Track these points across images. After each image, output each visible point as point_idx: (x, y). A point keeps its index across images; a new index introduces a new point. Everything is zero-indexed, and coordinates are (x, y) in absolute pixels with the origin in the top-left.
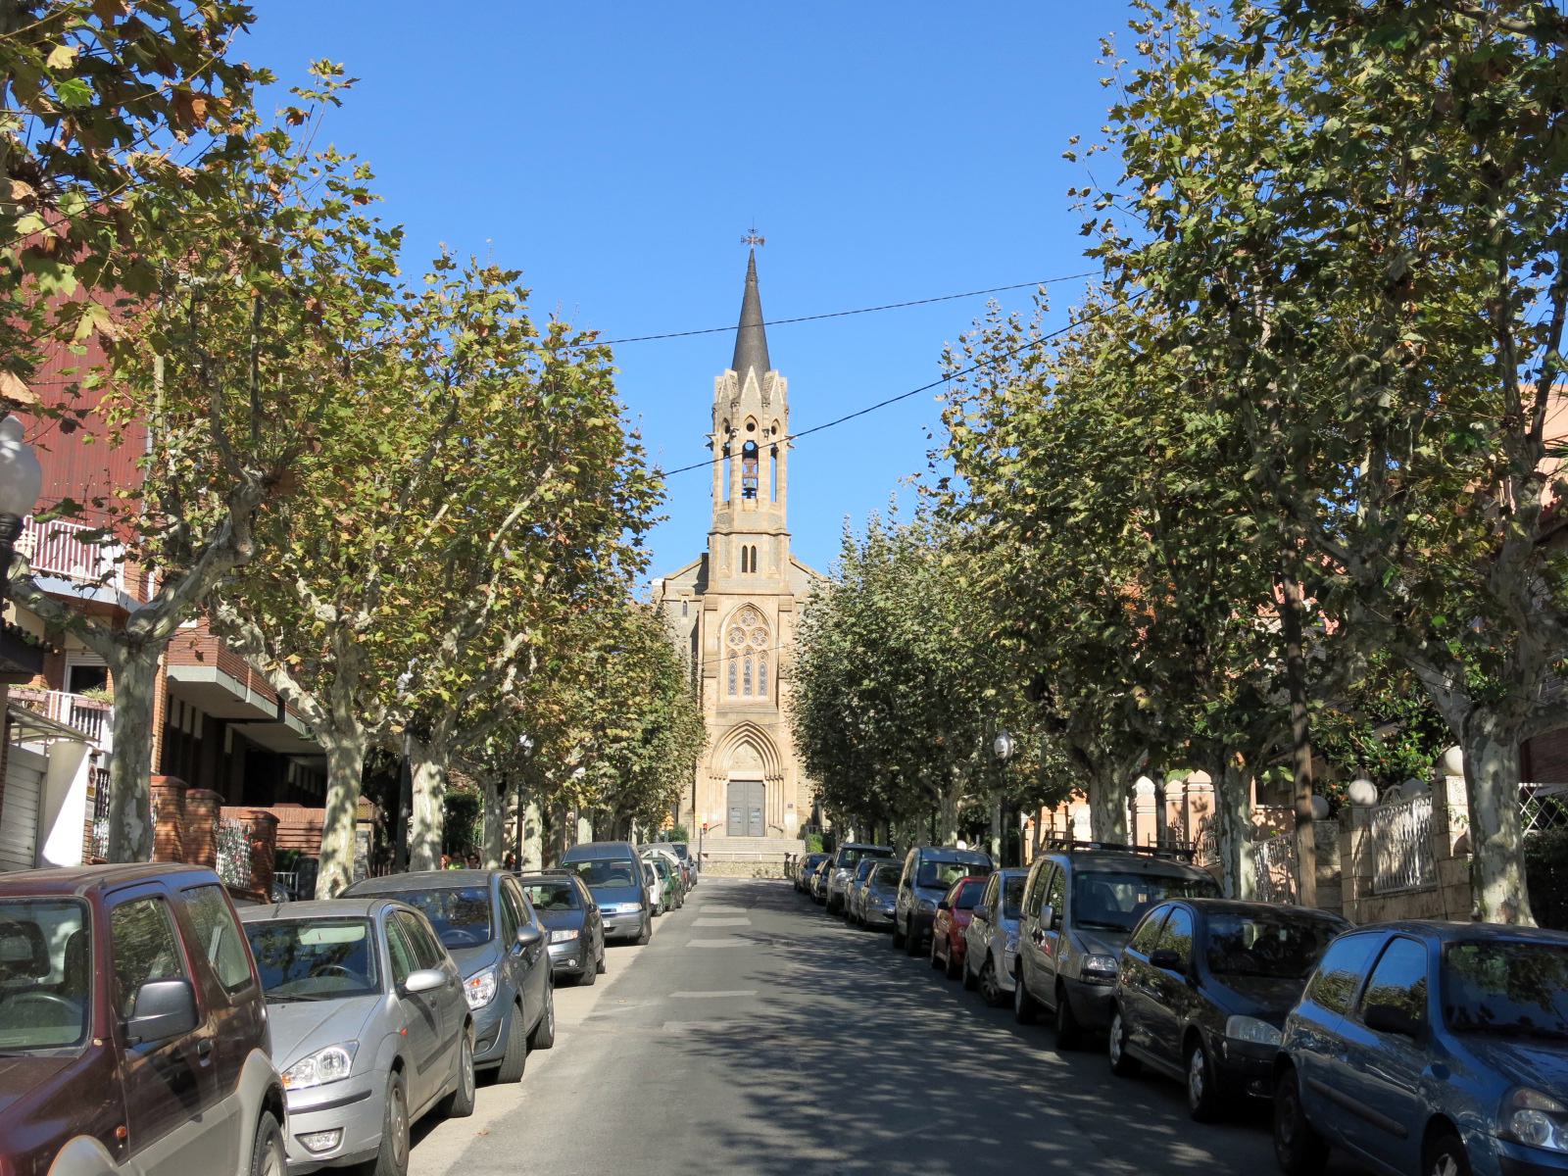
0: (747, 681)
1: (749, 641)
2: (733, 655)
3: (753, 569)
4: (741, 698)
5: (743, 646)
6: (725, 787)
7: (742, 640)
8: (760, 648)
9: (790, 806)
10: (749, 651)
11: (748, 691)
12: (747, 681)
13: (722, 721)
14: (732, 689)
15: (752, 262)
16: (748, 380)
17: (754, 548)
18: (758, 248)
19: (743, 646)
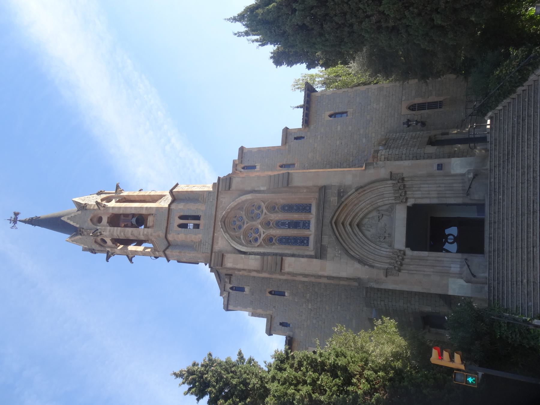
0: (295, 225)
1: (257, 224)
2: (270, 240)
3: (197, 218)
4: (311, 233)
5: (261, 230)
6: (416, 253)
7: (257, 231)
8: (265, 211)
9: (440, 167)
10: (267, 224)
11: (306, 225)
12: (295, 225)
13: (330, 252)
14: (303, 241)
15: (25, 222)
16: (69, 221)
17: (181, 218)
18: (20, 217)
19: (261, 230)
